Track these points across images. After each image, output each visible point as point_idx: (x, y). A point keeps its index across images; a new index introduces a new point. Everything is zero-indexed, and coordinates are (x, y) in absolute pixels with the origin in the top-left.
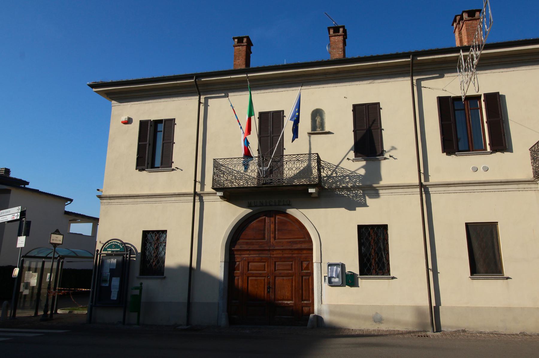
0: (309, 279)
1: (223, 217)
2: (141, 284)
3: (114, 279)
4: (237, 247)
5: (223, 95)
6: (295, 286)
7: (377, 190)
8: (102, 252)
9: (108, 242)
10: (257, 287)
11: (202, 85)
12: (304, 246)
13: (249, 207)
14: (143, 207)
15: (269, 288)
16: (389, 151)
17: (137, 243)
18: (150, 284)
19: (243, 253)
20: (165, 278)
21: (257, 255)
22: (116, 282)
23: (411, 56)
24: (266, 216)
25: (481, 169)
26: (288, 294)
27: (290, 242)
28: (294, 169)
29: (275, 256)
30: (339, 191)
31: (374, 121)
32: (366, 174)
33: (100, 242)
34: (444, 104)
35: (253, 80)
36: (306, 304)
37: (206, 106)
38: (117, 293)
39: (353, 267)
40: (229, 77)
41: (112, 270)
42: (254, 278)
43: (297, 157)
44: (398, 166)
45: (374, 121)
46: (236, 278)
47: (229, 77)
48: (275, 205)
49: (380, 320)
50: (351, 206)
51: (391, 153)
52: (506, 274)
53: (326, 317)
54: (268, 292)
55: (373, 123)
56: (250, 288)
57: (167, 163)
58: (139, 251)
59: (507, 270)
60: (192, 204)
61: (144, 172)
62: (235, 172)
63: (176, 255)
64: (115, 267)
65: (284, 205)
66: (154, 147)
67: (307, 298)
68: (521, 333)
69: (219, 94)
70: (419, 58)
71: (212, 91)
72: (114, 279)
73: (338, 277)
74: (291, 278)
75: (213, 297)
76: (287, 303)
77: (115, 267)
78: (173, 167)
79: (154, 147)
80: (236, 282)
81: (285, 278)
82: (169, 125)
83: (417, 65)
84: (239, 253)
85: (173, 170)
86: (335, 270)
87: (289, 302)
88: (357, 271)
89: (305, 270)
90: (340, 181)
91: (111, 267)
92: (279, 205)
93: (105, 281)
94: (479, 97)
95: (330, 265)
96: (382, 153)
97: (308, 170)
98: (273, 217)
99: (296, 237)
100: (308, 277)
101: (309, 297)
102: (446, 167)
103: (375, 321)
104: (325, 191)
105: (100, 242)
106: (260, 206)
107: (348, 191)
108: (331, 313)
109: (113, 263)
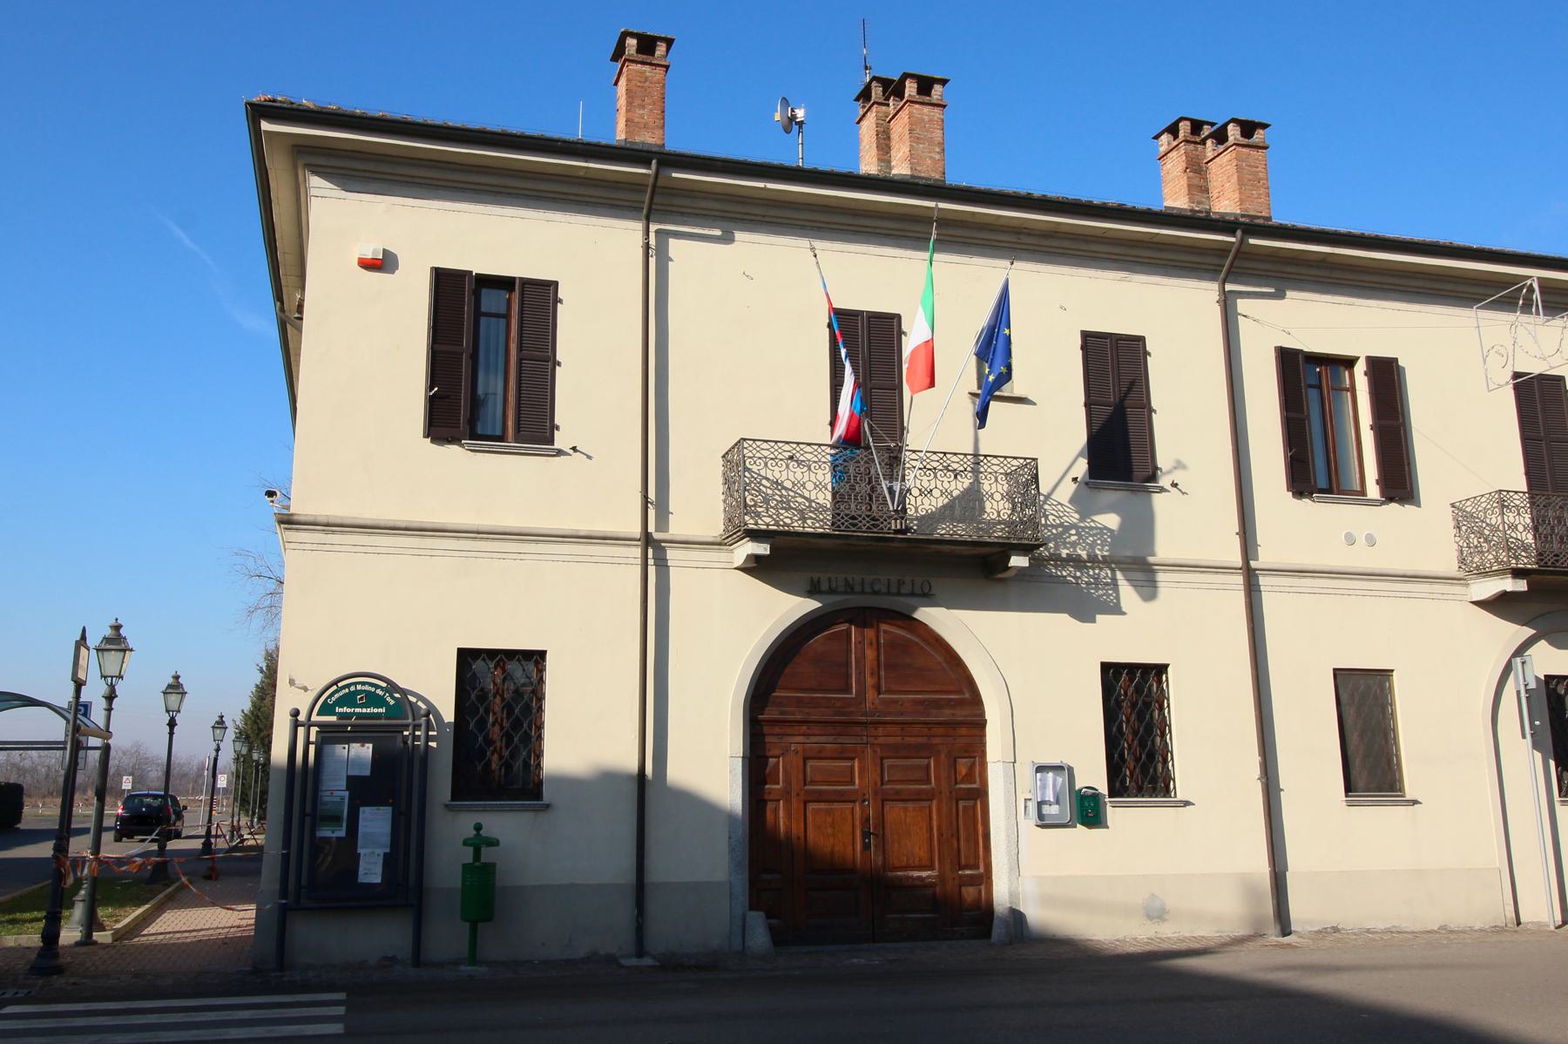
0: (974, 807)
1: (736, 620)
2: (478, 827)
3: (366, 813)
4: (770, 713)
5: (718, 233)
6: (939, 828)
7: (1154, 572)
8: (314, 718)
9: (335, 683)
10: (834, 833)
11: (667, 190)
12: (961, 714)
13: (812, 592)
14: (491, 564)
15: (866, 834)
16: (1169, 472)
17: (438, 691)
18: (505, 825)
19: (789, 731)
20: (548, 806)
21: (831, 739)
22: (376, 823)
23: (1239, 233)
24: (851, 622)
25: (1361, 539)
26: (921, 852)
27: (922, 702)
28: (936, 493)
29: (881, 740)
30: (1056, 567)
31: (1132, 384)
32: (1122, 526)
33: (292, 682)
34: (1292, 364)
35: (946, 221)
36: (971, 876)
37: (664, 260)
38: (380, 861)
39: (1093, 775)
40: (761, 185)
41: (353, 782)
42: (822, 806)
43: (942, 463)
44: (1189, 513)
45: (1132, 384)
46: (770, 806)
47: (761, 185)
48: (889, 593)
49: (1157, 914)
50: (1086, 608)
51: (1177, 476)
52: (1410, 793)
53: (1037, 915)
54: (866, 847)
55: (1129, 390)
56: (812, 835)
57: (534, 426)
58: (449, 715)
59: (1412, 782)
60: (638, 570)
61: (454, 448)
62: (764, 482)
63: (582, 734)
64: (367, 773)
65: (913, 594)
66: (487, 367)
67: (972, 861)
68: (1441, 928)
69: (684, 224)
70: (1252, 241)
71: (682, 214)
72: (366, 813)
73: (1057, 802)
74: (926, 804)
75: (705, 867)
76: (920, 878)
77: (367, 773)
78: (561, 440)
79: (487, 367)
80: (769, 816)
81: (910, 805)
82: (536, 301)
83: (1246, 255)
84: (777, 730)
85: (560, 453)
86: (1050, 783)
87: (924, 874)
88: (1103, 788)
89: (962, 782)
90: (1056, 537)
91: (353, 772)
92: (899, 594)
93: (335, 819)
94: (1349, 362)
95: (1041, 769)
96: (1153, 477)
97: (972, 500)
98: (871, 626)
99: (937, 688)
100: (971, 803)
101: (977, 857)
102: (1295, 527)
103: (1150, 917)
104: (987, 565)
105: (292, 682)
106: (846, 593)
107: (1077, 568)
108: (1047, 900)
109: (357, 762)
